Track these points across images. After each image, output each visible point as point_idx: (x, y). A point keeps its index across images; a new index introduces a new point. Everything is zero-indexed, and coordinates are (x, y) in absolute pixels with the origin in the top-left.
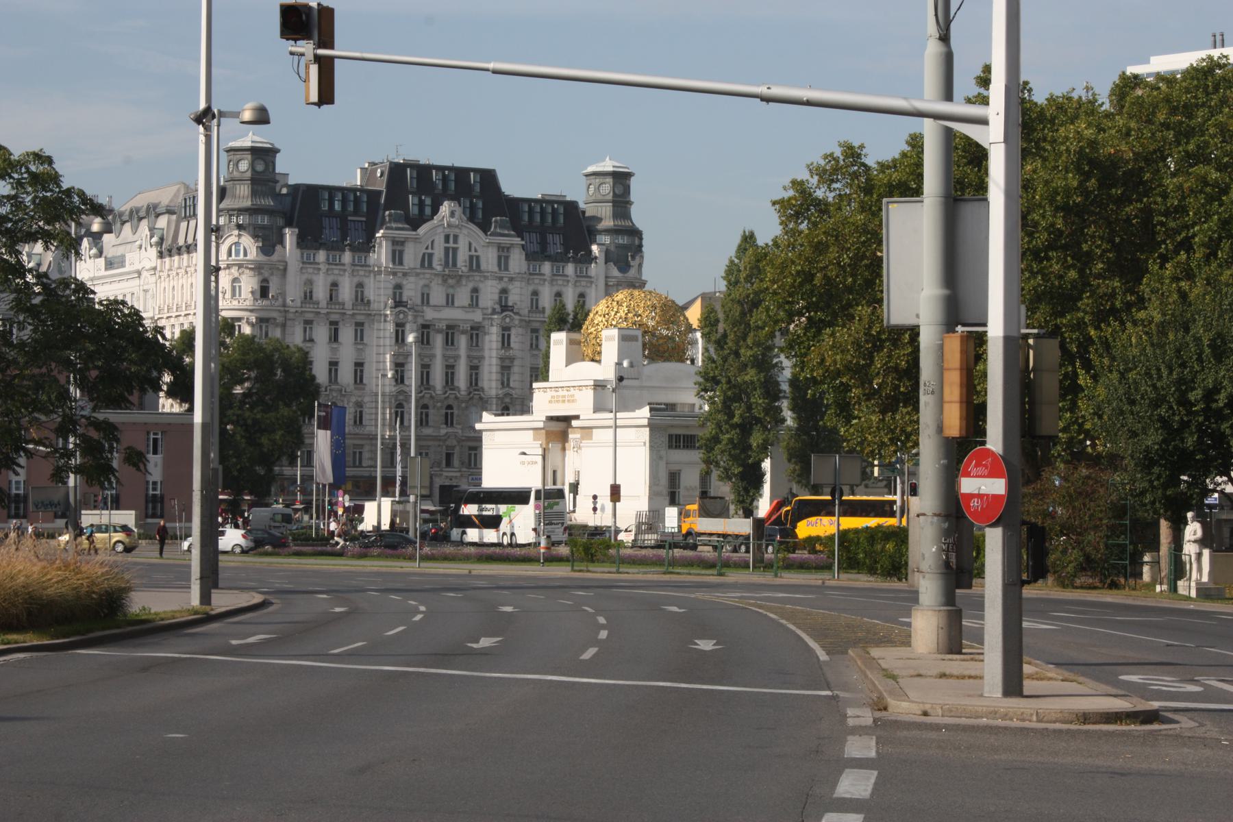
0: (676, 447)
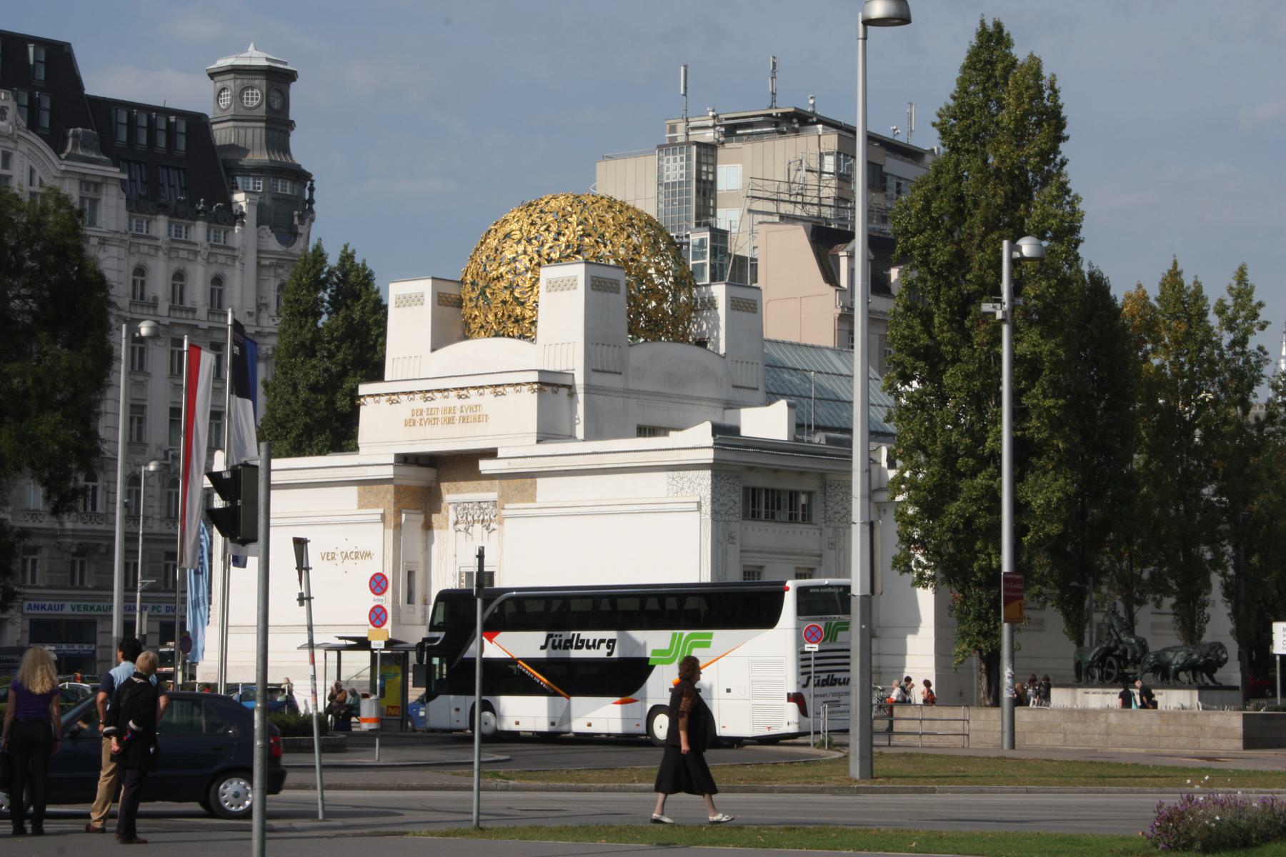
0: (753, 516)
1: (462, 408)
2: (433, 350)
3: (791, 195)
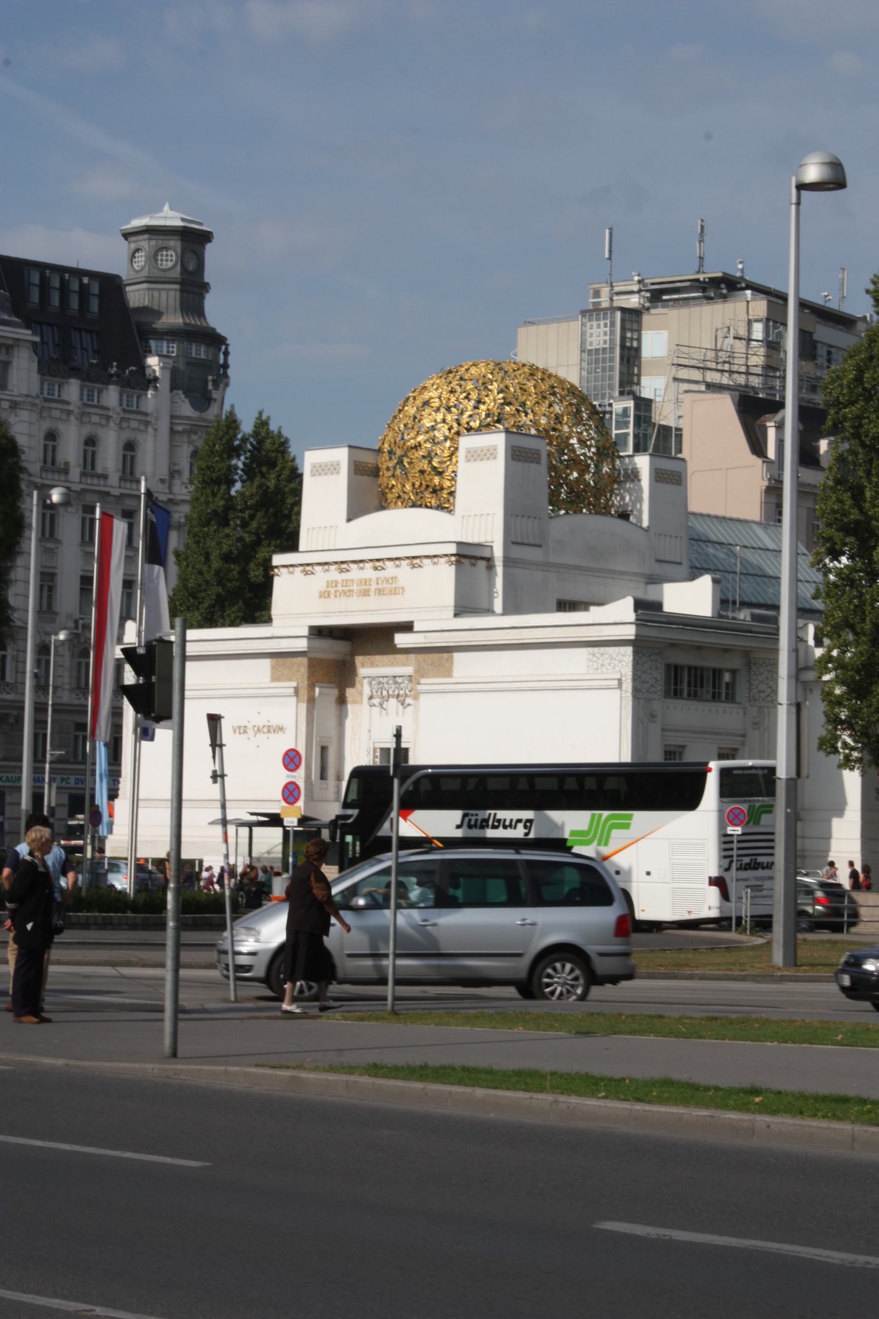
0: (675, 693)
1: (377, 579)
2: (349, 520)
3: (717, 363)
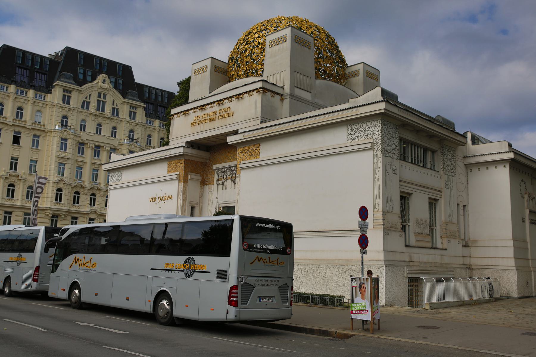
1: (220, 110)
